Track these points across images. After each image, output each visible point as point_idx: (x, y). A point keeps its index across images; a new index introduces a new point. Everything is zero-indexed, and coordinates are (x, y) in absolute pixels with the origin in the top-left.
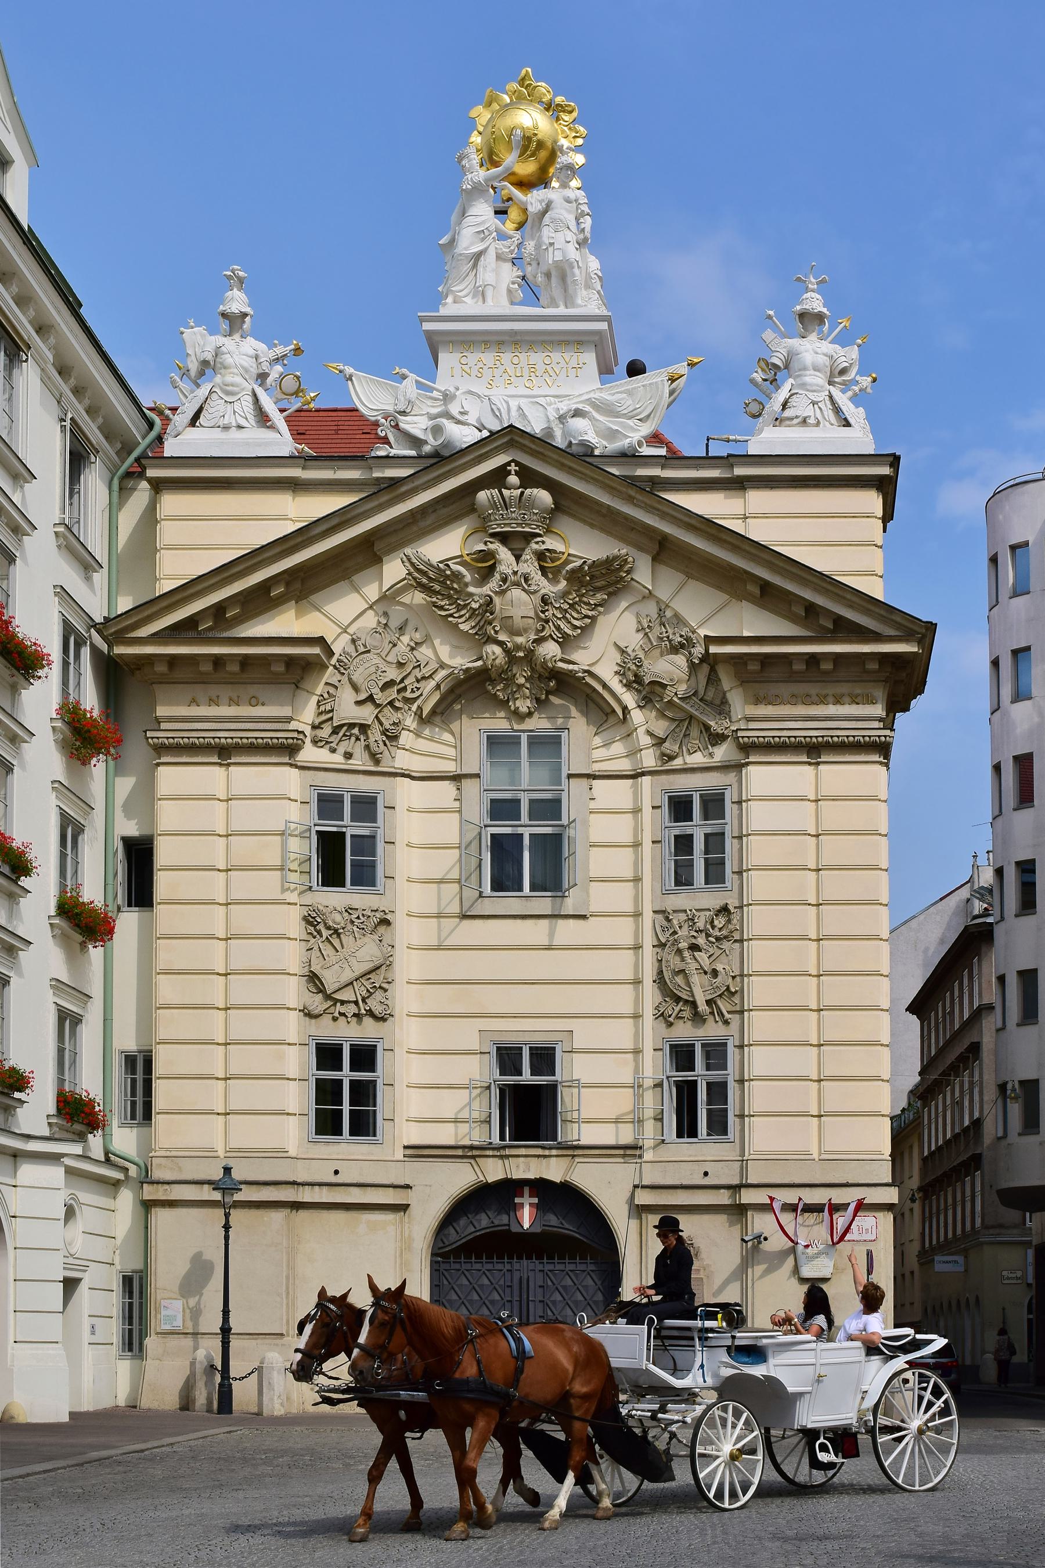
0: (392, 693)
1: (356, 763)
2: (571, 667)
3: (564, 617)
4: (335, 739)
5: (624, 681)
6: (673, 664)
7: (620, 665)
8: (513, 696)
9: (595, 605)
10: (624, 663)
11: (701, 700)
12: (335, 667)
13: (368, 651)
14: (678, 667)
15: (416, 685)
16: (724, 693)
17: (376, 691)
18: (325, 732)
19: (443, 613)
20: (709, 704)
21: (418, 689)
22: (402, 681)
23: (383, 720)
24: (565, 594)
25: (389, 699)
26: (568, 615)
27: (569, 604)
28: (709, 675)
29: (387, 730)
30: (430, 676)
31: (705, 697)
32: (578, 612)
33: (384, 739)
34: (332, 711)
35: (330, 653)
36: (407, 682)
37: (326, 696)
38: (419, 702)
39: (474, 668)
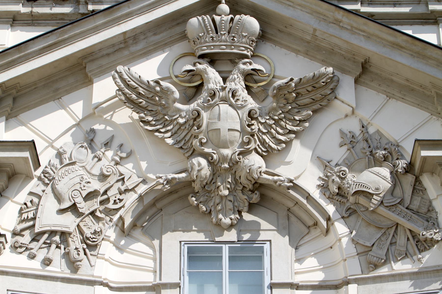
0: (94, 204)
1: (54, 270)
2: (276, 178)
3: (269, 132)
4: (34, 245)
5: (327, 194)
6: (378, 174)
7: (323, 180)
8: (215, 208)
9: (300, 121)
10: (327, 176)
11: (407, 208)
12: (40, 179)
13: (74, 163)
14: (384, 178)
15: (118, 196)
16: (430, 202)
17: (79, 200)
18: (26, 238)
19: (150, 128)
20: (417, 213)
21: (121, 200)
22: (105, 192)
23: (85, 229)
24: (270, 113)
25: (92, 210)
26: (272, 131)
27: (274, 119)
28: (415, 185)
29: (88, 239)
30: (133, 189)
31: (411, 207)
32: (282, 128)
33: (85, 246)
34: (34, 219)
35: (37, 164)
36: (110, 193)
37: (29, 204)
38: (121, 212)
39: (179, 179)
